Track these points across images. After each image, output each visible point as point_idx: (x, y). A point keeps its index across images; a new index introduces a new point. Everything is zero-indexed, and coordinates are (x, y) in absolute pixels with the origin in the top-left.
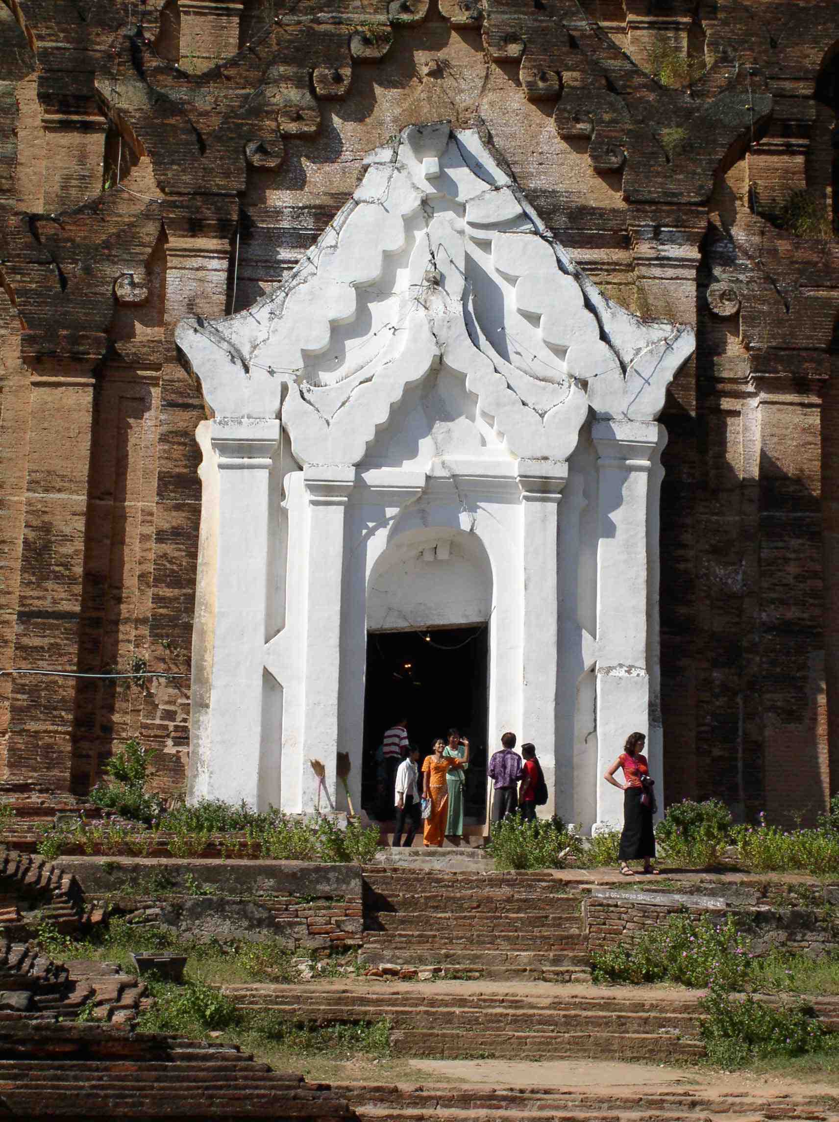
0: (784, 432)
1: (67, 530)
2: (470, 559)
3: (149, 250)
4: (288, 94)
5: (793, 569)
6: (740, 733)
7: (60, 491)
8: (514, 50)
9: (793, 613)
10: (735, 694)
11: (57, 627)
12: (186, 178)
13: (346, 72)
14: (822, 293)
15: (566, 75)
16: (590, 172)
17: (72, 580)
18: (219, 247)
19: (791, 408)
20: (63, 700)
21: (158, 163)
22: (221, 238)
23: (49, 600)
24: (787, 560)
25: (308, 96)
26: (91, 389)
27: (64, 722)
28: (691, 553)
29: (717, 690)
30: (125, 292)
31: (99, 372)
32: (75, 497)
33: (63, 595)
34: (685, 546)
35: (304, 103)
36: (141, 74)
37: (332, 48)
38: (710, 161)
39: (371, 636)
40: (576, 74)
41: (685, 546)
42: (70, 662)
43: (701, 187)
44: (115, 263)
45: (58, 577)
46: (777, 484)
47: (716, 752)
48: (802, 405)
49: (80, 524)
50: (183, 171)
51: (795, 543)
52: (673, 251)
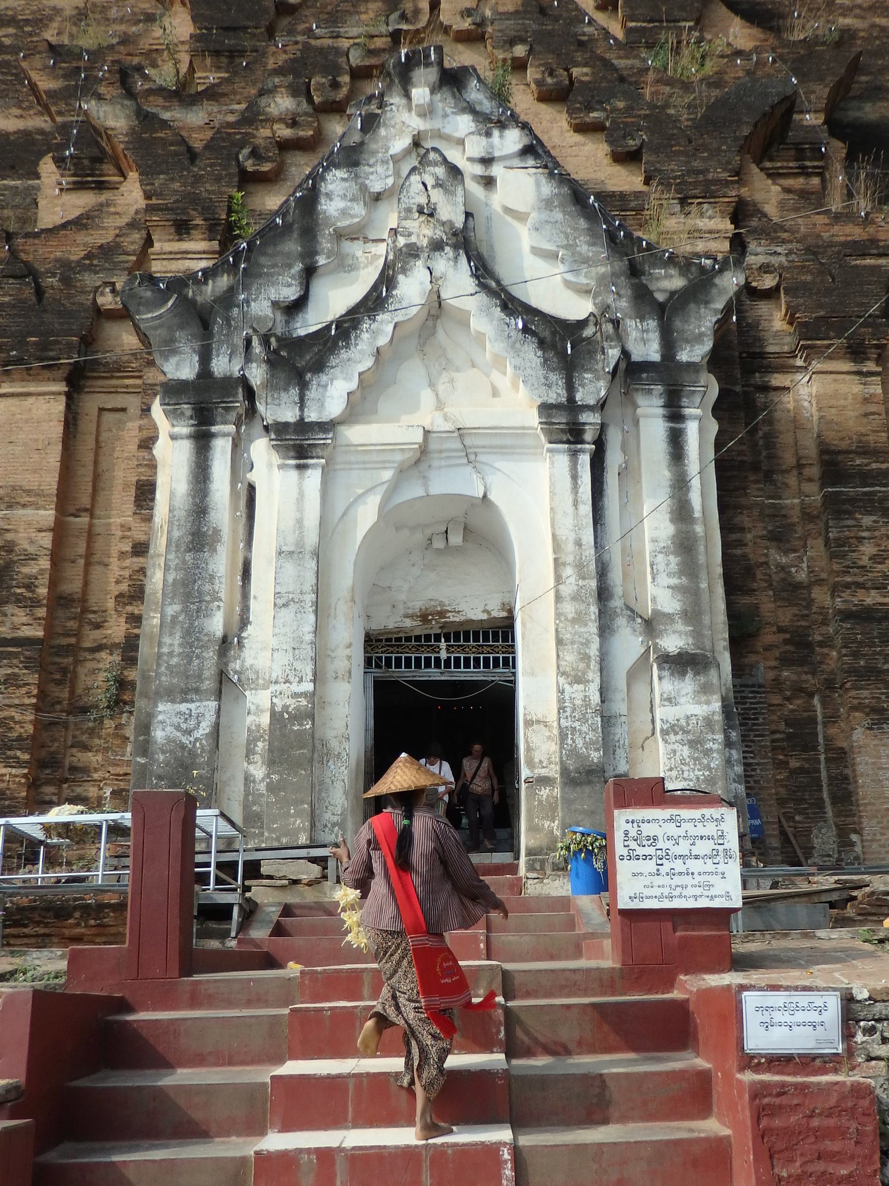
0: (843, 402)
1: (31, 549)
2: (474, 532)
3: (134, 258)
4: (283, 103)
5: (868, 549)
6: (821, 739)
7: (24, 506)
8: (520, 50)
9: (872, 598)
10: (811, 695)
11: (15, 655)
12: (176, 185)
13: (346, 79)
14: (869, 261)
15: (576, 72)
16: (607, 160)
17: (35, 603)
18: (206, 249)
19: (848, 377)
20: (20, 738)
21: (147, 174)
22: (211, 240)
23: (8, 624)
24: (860, 539)
25: (305, 105)
26: (63, 399)
27: (20, 764)
28: (749, 536)
29: (788, 693)
30: (107, 300)
31: (77, 381)
32: (42, 512)
33: (25, 619)
34: (742, 530)
35: (299, 110)
36: (130, 93)
37: (328, 61)
38: (736, 139)
39: (371, 641)
40: (585, 70)
41: (742, 530)
42: (29, 694)
43: (729, 162)
44: (96, 273)
45: (19, 601)
46: (840, 458)
47: (794, 764)
48: (859, 373)
49: (46, 540)
50: (172, 179)
51: (867, 520)
52: (704, 223)
